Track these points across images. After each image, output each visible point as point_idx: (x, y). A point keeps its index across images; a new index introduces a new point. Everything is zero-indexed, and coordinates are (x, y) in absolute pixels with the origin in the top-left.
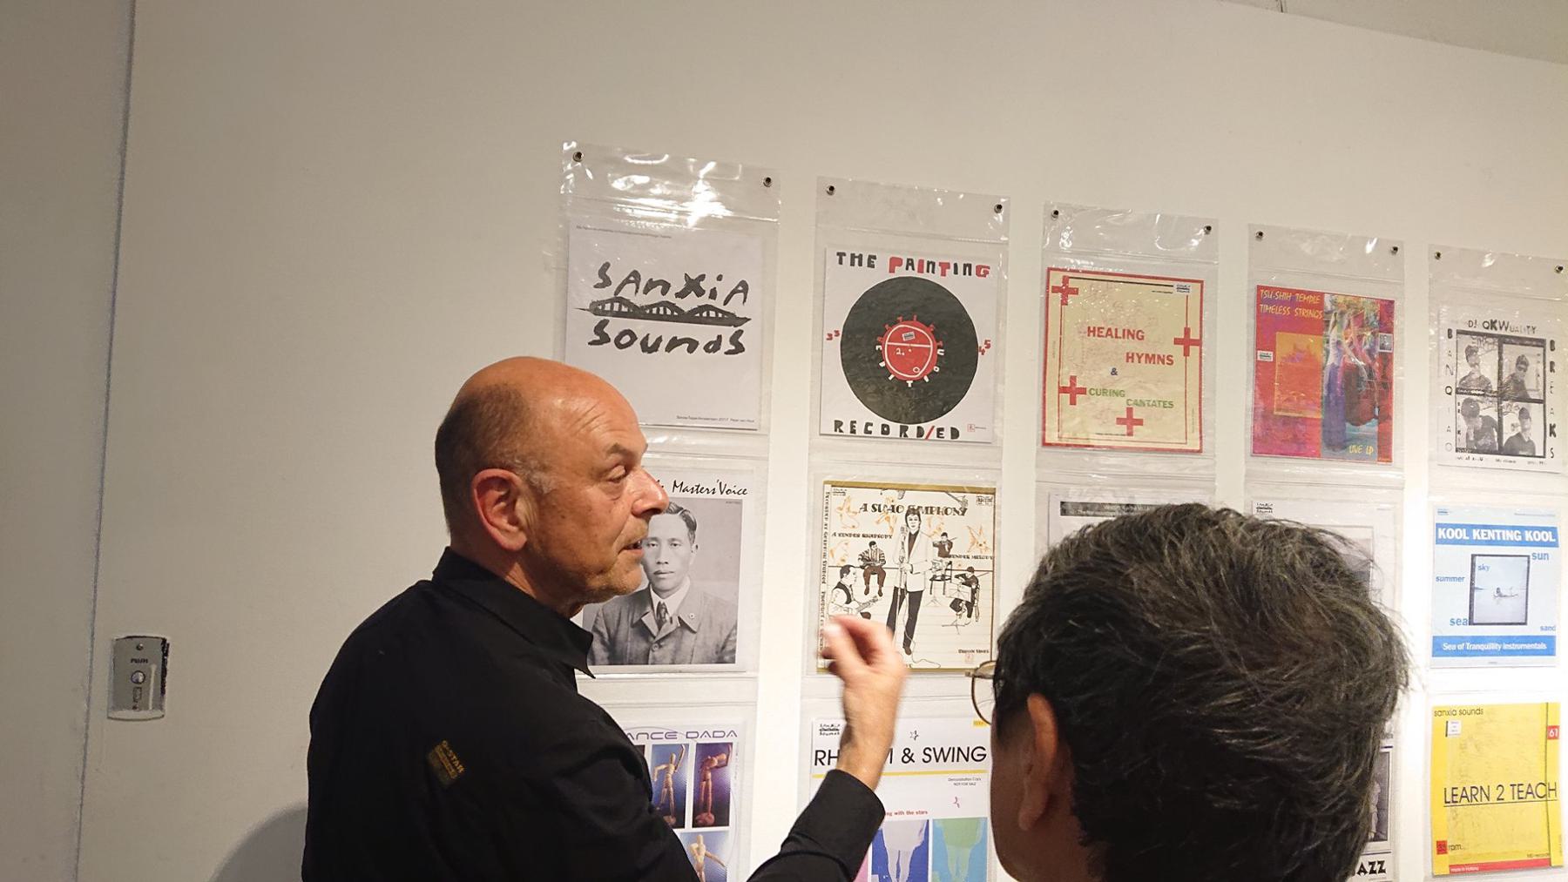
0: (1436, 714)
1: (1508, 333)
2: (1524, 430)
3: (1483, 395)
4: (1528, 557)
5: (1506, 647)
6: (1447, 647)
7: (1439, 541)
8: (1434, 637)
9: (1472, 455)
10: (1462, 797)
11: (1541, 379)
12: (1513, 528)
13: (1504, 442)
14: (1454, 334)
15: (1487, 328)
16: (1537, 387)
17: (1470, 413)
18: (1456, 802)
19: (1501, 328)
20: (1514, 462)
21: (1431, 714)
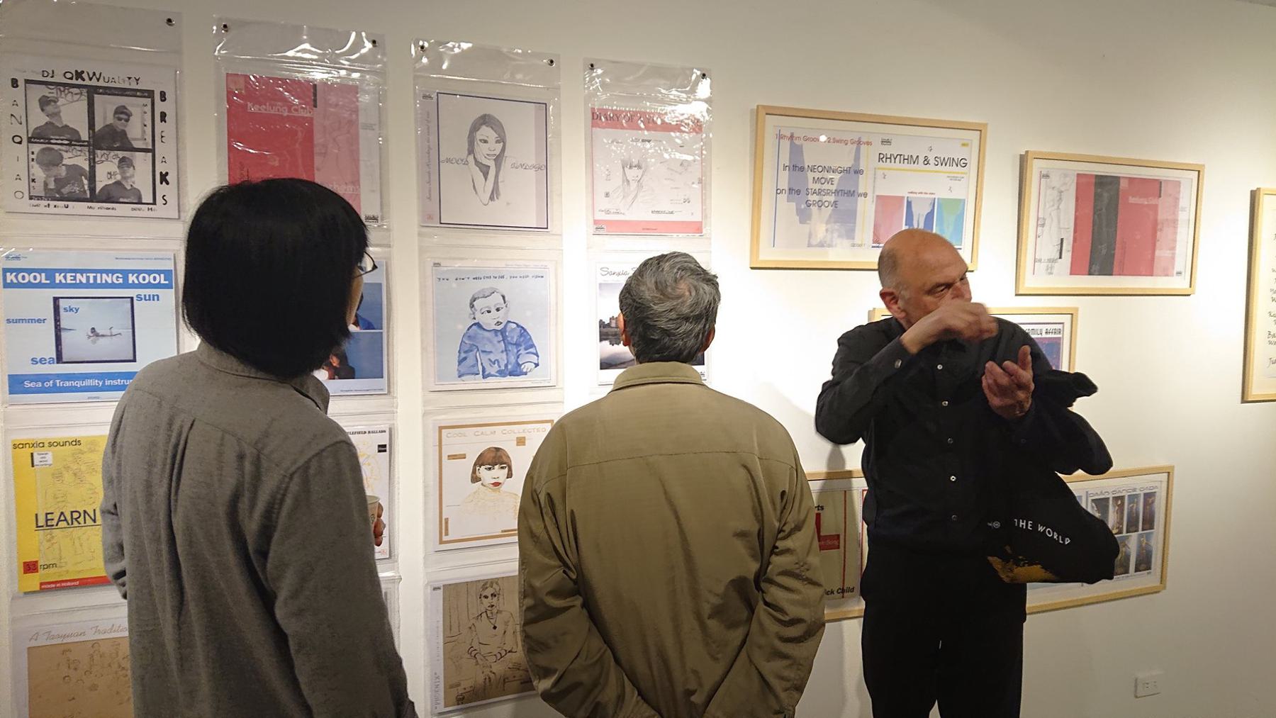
0: (15, 446)
1: (101, 83)
2: (125, 178)
3: (70, 145)
4: (132, 298)
5: (108, 383)
6: (28, 384)
7: (6, 285)
8: (601, 369)
9: (53, 203)
10: (59, 520)
11: (149, 130)
12: (113, 272)
13: (97, 191)
14: (21, 83)
15: (71, 79)
16: (143, 135)
17: (49, 161)
18: (53, 526)
19: (91, 79)
20: (113, 209)
21: (11, 447)
